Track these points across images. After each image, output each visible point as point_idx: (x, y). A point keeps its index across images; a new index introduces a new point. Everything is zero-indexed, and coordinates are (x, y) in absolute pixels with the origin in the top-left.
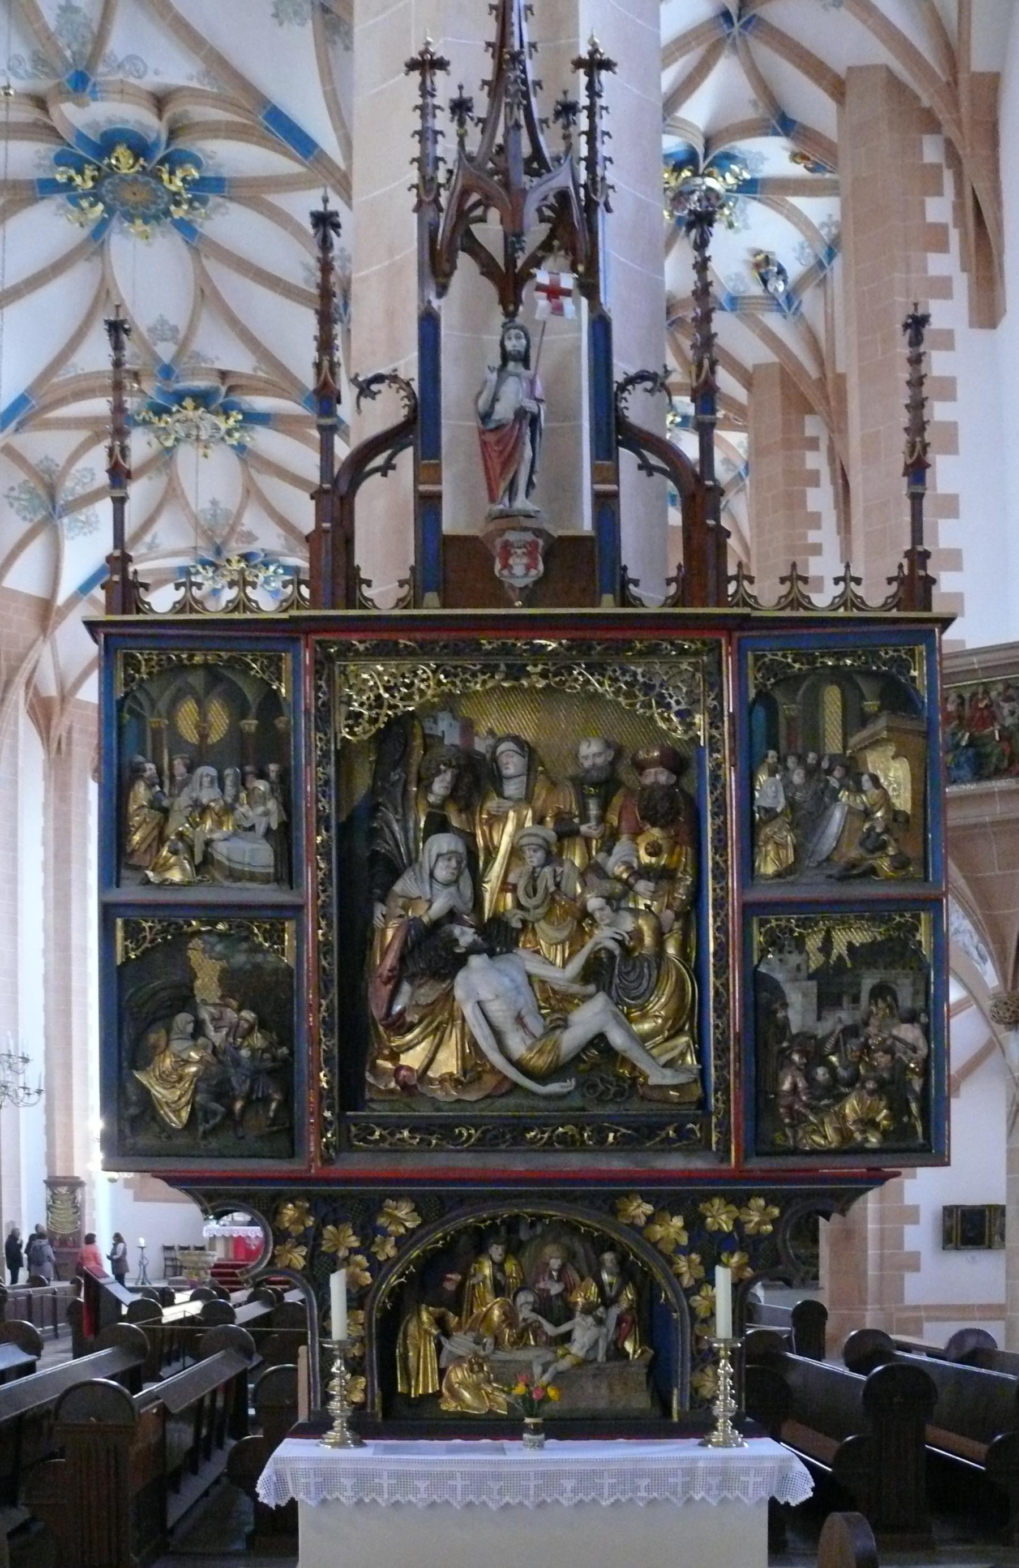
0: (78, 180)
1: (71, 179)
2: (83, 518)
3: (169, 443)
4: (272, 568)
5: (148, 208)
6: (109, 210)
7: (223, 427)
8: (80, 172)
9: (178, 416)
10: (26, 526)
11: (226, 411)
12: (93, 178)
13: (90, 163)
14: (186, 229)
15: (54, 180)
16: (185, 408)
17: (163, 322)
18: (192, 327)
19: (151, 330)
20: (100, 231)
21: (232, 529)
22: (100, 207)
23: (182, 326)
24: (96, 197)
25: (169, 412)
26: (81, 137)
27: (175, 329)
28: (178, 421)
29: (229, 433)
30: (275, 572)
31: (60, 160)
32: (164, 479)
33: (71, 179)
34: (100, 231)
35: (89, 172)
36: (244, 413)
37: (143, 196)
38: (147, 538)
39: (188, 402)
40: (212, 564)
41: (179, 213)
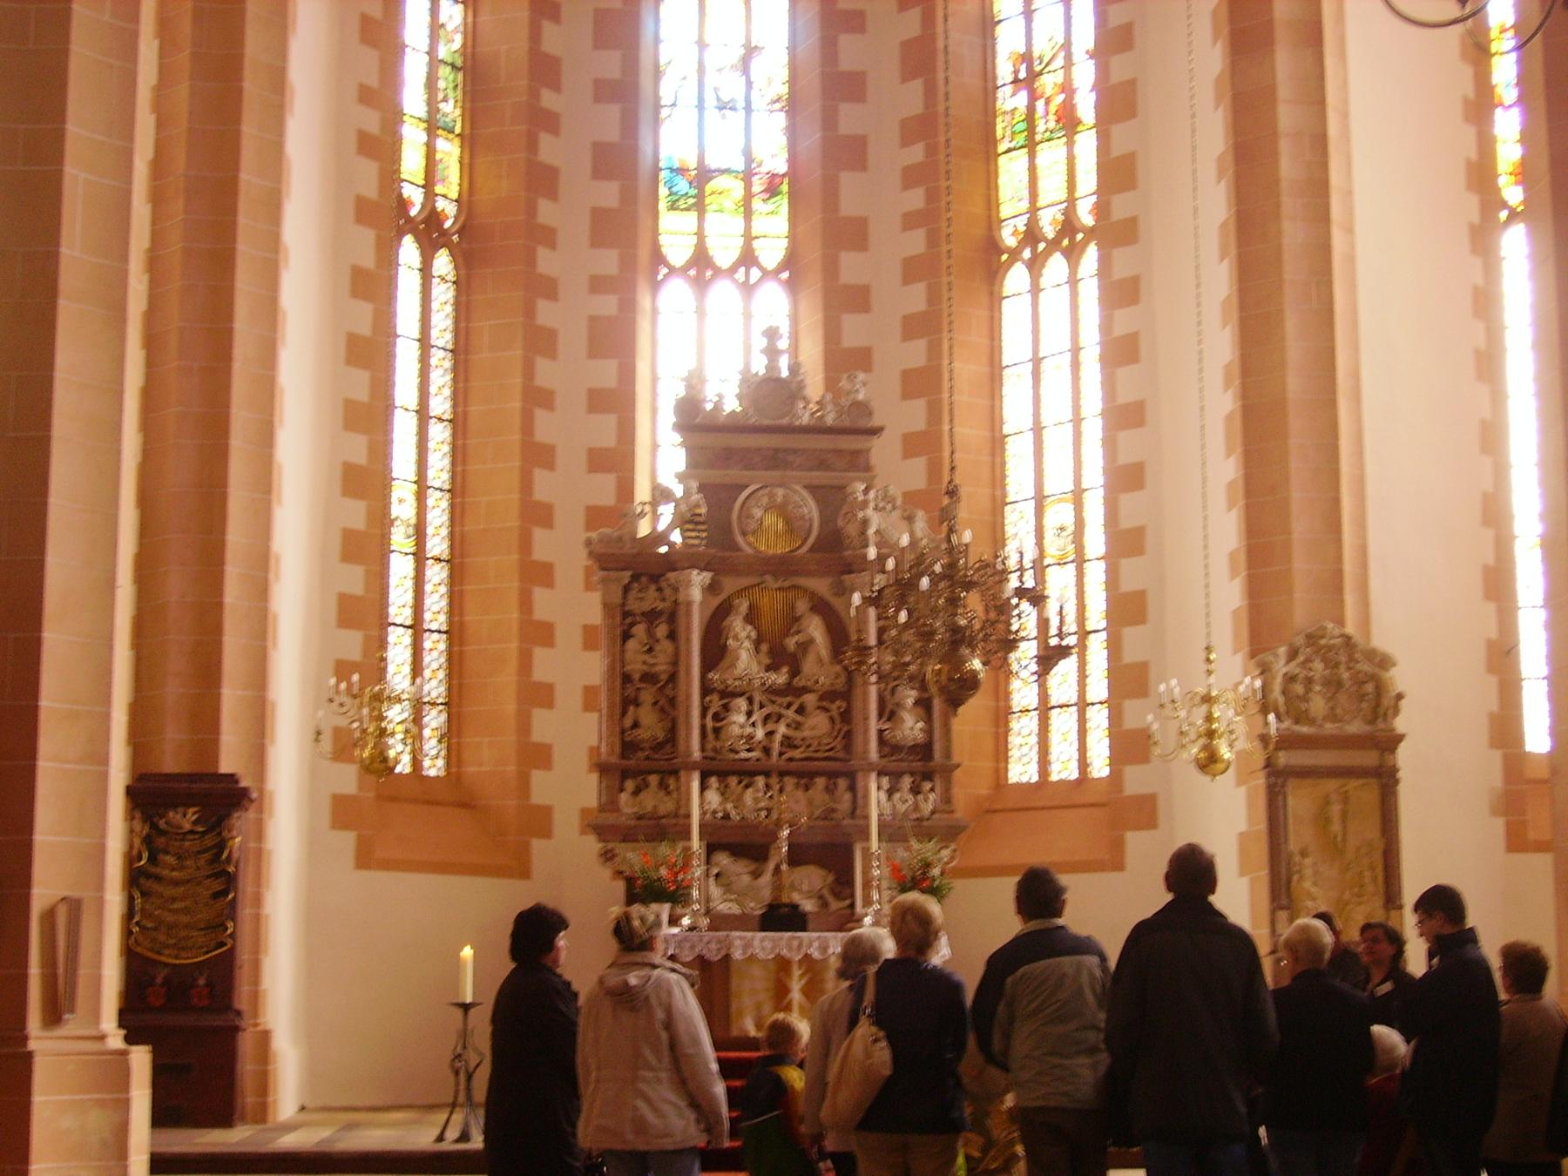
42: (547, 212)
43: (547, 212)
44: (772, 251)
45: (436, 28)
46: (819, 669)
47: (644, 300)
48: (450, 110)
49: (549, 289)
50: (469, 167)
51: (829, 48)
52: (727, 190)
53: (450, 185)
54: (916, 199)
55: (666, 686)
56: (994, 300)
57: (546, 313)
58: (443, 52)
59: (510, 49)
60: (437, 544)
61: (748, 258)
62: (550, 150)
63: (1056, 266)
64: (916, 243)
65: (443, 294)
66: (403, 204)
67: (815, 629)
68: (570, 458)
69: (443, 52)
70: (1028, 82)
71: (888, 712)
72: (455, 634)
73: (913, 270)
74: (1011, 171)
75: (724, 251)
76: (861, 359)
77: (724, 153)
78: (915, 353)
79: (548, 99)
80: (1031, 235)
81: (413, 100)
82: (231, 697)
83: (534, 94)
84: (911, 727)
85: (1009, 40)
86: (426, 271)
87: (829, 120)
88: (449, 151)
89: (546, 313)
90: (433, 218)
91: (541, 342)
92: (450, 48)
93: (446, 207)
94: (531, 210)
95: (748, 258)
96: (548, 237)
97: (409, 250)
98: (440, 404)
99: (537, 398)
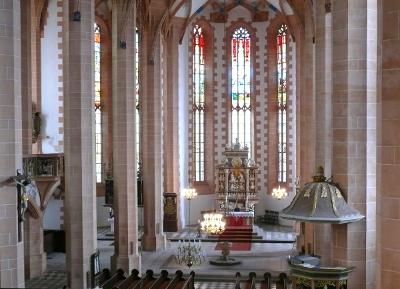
42: (216, 104)
43: (216, 104)
44: (248, 105)
46: (242, 180)
47: (230, 114)
48: (203, 90)
49: (216, 114)
51: (255, 78)
52: (241, 96)
53: (203, 100)
54: (266, 100)
55: (224, 182)
56: (278, 117)
57: (216, 118)
59: (210, 80)
60: (202, 150)
61: (245, 106)
62: (216, 95)
63: (285, 111)
64: (266, 107)
65: (202, 116)
67: (242, 176)
68: (220, 137)
70: (282, 83)
71: (250, 185)
72: (205, 162)
73: (266, 110)
74: (280, 96)
75: (241, 105)
76: (259, 123)
77: (241, 91)
78: (266, 122)
80: (282, 105)
81: (197, 91)
82: (175, 183)
84: (253, 187)
85: (280, 76)
87: (255, 88)
88: (202, 96)
89: (216, 118)
90: (200, 106)
91: (215, 122)
92: (202, 81)
95: (245, 106)
96: (216, 107)
98: (202, 131)
99: (215, 130)
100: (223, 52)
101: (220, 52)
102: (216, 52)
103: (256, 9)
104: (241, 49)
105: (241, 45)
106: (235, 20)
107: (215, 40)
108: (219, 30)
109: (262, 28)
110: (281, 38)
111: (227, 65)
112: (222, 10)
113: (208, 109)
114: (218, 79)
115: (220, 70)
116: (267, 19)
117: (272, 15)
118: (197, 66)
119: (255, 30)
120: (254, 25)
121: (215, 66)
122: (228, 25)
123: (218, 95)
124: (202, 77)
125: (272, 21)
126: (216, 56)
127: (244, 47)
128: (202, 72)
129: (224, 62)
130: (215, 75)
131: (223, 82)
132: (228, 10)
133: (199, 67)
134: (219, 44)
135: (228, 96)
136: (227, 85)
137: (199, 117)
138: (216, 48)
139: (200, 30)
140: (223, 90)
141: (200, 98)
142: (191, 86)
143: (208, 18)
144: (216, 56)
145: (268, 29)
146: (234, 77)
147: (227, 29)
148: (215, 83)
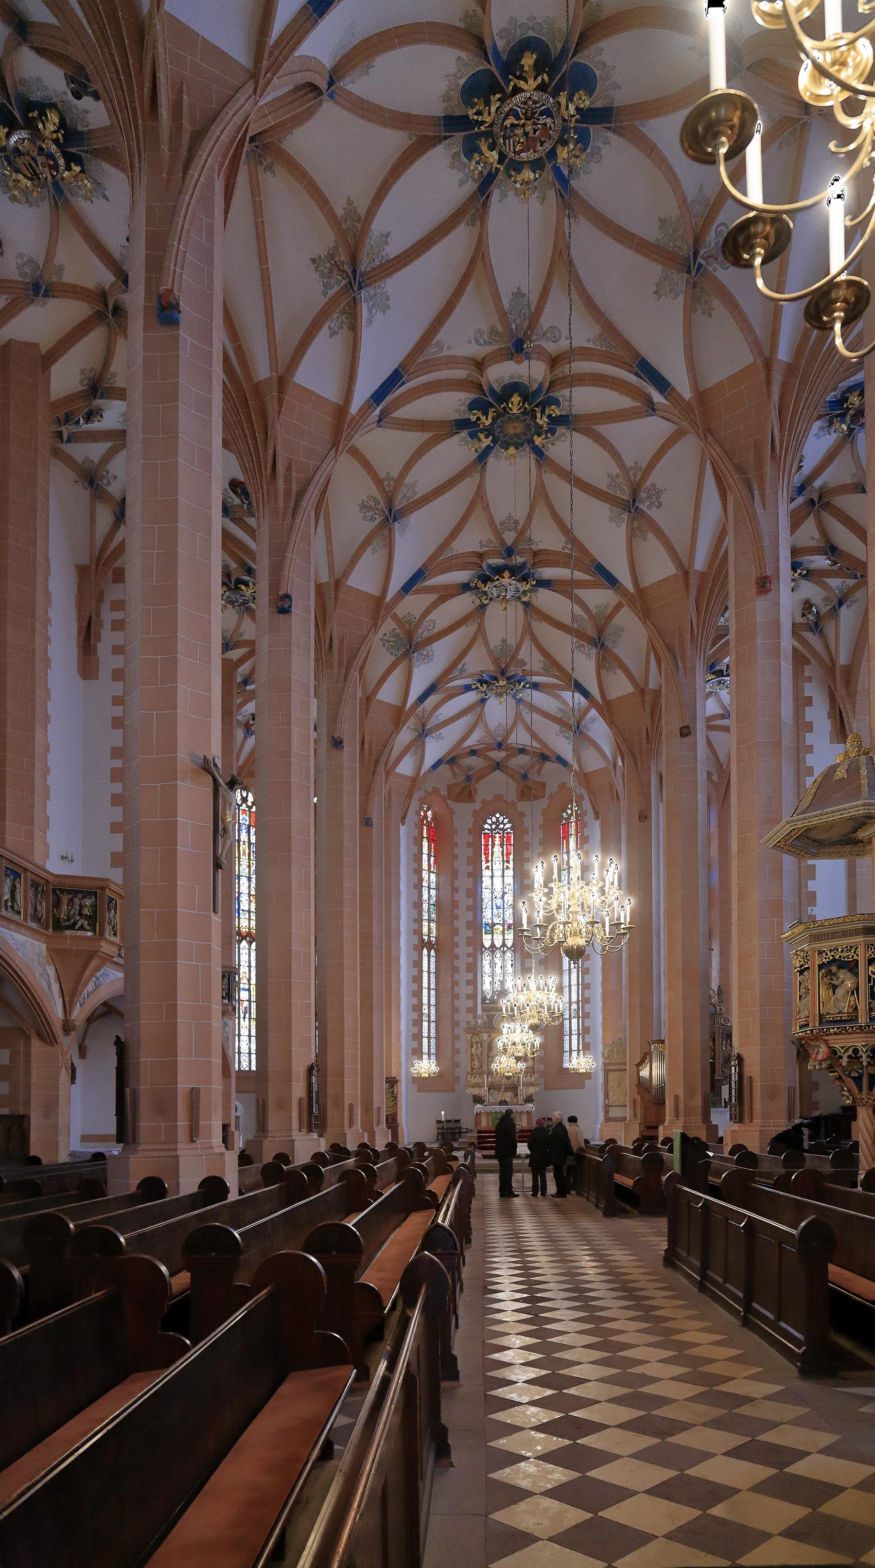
0: (483, 418)
1: (479, 419)
2: (425, 653)
3: (486, 602)
4: (522, 684)
5: (519, 438)
6: (495, 441)
7: (521, 590)
8: (486, 414)
9: (496, 583)
10: (393, 658)
11: (524, 579)
12: (493, 418)
13: (493, 406)
14: (539, 452)
15: (469, 419)
16: (503, 577)
17: (510, 517)
18: (529, 519)
19: (502, 523)
20: (483, 457)
21: (513, 657)
22: (491, 438)
23: (522, 518)
24: (489, 431)
25: (493, 581)
26: (492, 390)
27: (517, 523)
28: (495, 586)
29: (525, 593)
30: (524, 687)
31: (472, 406)
32: (476, 626)
33: (479, 419)
34: (483, 457)
35: (490, 415)
36: (537, 581)
37: (519, 428)
38: (460, 666)
39: (506, 574)
40: (486, 682)
41: (538, 441)
42: (456, 939)
43: (456, 939)
45: (430, 896)
48: (433, 916)
50: (438, 929)
58: (431, 902)
66: (423, 940)
69: (431, 902)
79: (456, 911)
81: (425, 916)
83: (453, 911)
86: (429, 956)
88: (433, 925)
93: (433, 939)
94: (452, 939)
97: (425, 952)
100: (470, 852)
101: (463, 852)
102: (456, 851)
103: (525, 776)
104: (497, 849)
105: (497, 841)
106: (490, 798)
107: (455, 831)
108: (463, 814)
109: (534, 811)
110: (566, 828)
111: (476, 876)
112: (468, 779)
113: (440, 947)
114: (460, 896)
115: (464, 883)
116: (543, 796)
117: (552, 788)
118: (425, 874)
119: (522, 815)
120: (523, 806)
121: (454, 874)
122: (477, 805)
123: (460, 924)
124: (433, 893)
125: (551, 797)
126: (456, 857)
127: (502, 845)
128: (433, 885)
129: (470, 869)
130: (455, 890)
131: (470, 901)
132: (479, 779)
133: (430, 878)
134: (462, 838)
135: (477, 926)
136: (476, 908)
137: (428, 961)
138: (456, 845)
139: (429, 813)
140: (469, 916)
141: (429, 929)
142: (418, 905)
143: (444, 792)
144: (456, 857)
145: (545, 812)
146: (486, 894)
147: (475, 814)
148: (455, 904)
